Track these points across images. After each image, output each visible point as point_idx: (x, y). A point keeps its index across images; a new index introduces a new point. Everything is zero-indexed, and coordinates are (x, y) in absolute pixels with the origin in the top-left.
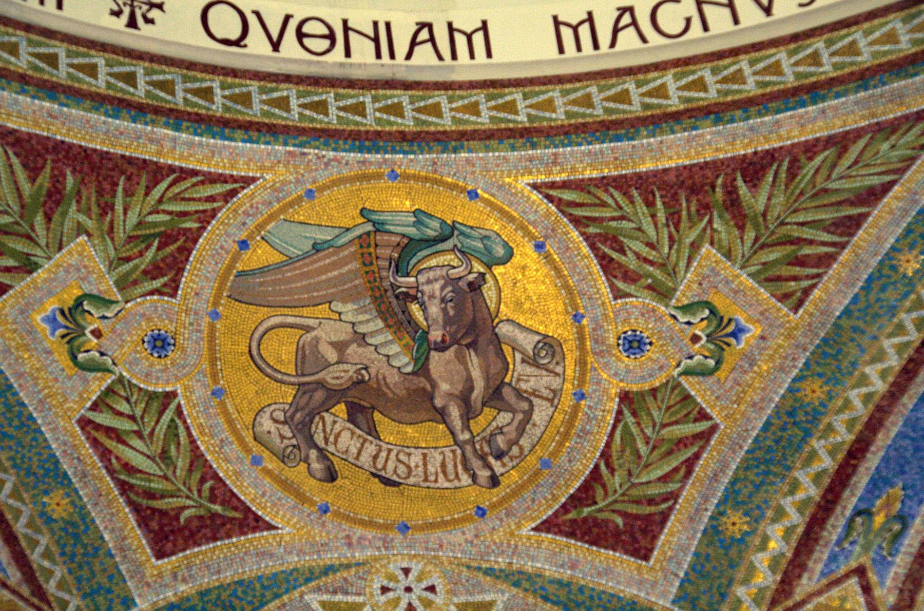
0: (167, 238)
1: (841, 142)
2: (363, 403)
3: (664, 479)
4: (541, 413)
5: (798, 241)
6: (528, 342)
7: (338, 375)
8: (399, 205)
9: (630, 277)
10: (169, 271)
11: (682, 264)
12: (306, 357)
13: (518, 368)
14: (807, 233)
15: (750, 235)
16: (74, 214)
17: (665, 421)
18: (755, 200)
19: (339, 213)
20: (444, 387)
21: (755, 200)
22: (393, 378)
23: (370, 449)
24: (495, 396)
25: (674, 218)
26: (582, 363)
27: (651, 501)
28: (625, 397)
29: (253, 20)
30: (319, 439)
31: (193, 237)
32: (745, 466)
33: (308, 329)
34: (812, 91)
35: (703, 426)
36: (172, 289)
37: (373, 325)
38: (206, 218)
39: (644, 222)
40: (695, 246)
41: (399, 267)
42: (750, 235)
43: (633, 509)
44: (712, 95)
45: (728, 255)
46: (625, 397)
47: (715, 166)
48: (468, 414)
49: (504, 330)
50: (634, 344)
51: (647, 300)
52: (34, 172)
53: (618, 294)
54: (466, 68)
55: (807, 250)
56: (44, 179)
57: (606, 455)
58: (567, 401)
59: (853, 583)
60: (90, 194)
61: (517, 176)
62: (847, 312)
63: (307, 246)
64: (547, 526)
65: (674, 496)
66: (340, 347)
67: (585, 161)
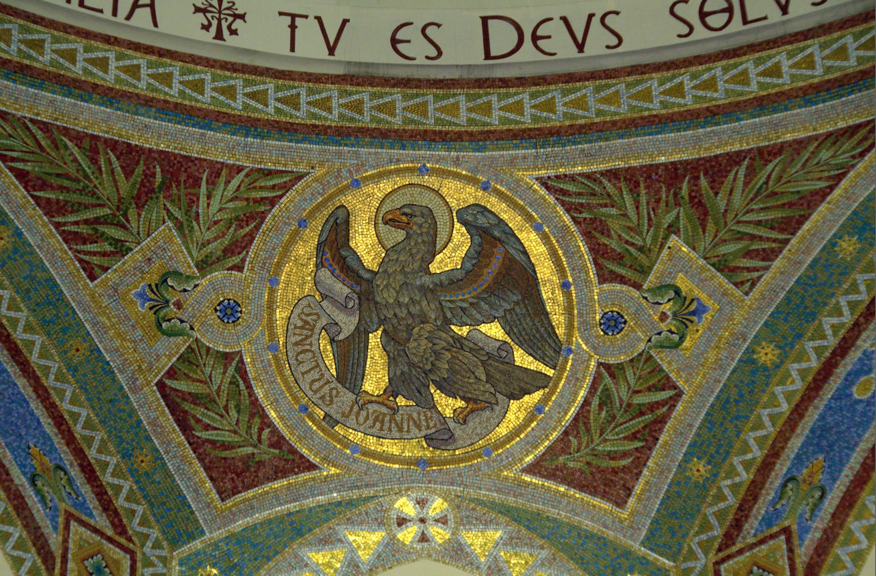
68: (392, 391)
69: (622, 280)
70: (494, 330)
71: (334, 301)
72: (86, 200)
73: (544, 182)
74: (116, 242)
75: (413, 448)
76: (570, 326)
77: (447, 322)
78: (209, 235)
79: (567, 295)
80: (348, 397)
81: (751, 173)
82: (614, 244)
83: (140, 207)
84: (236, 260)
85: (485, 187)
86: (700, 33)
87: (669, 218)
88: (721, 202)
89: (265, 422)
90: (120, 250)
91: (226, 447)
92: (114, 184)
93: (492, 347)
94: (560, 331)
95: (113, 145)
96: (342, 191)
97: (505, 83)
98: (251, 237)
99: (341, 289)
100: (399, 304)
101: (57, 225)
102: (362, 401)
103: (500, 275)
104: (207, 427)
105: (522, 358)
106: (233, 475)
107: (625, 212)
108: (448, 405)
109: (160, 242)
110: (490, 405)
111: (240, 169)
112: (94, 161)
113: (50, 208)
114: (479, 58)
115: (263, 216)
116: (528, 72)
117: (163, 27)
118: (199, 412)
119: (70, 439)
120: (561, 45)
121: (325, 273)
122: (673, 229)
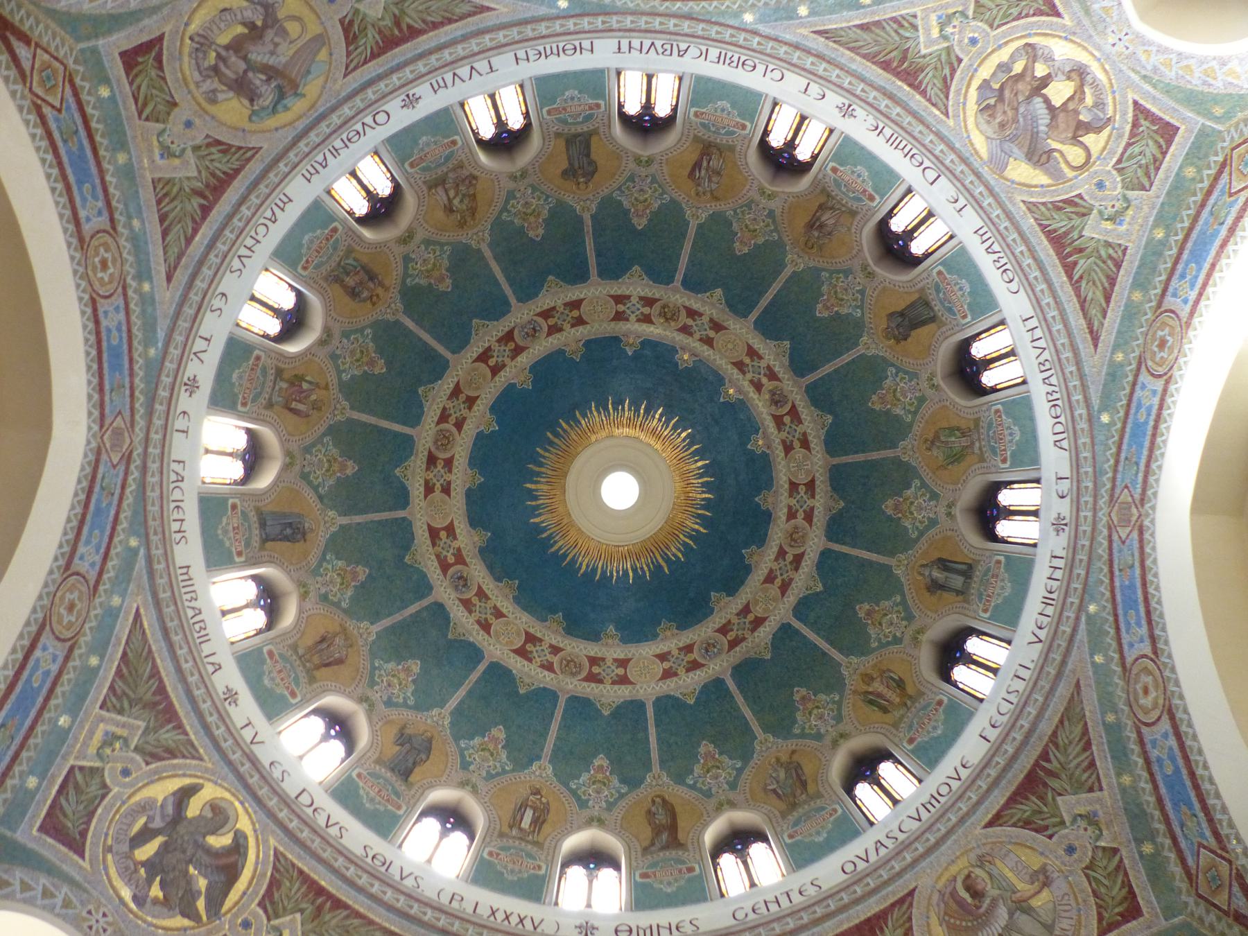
0: (355, 37)
1: (189, 241)
2: (255, 32)
3: (139, 87)
5: (172, 201)
6: (221, 96)
7: (270, 34)
8: (297, 106)
9: (208, 145)
10: (347, 26)
12: (283, 32)
13: (216, 84)
14: (172, 206)
15: (187, 190)
16: (388, 22)
17: (156, 107)
18: (196, 202)
19: (311, 88)
20: (233, 59)
21: (196, 202)
22: (251, 48)
23: (239, 17)
24: (215, 69)
25: (213, 175)
26: (199, 104)
27: (136, 76)
28: (175, 104)
29: (373, 125)
30: (259, 8)
31: (348, 45)
32: (119, 114)
33: (291, 42)
34: (211, 246)
35: (144, 116)
36: (342, 21)
37: (272, 61)
38: (348, 54)
39: (222, 164)
40: (200, 172)
41: (279, 87)
42: (187, 190)
43: (140, 67)
44: (235, 220)
45: (188, 178)
46: (175, 104)
47: (216, 200)
48: (219, 56)
49: (231, 94)
51: (198, 142)
52: (409, 27)
53: (207, 136)
54: (305, 167)
55: (167, 200)
56: (405, 28)
57: (164, 79)
58: (192, 87)
59: (57, 104)
60: (387, 33)
61: (269, 146)
62: (137, 192)
63: (312, 70)
64: (161, 38)
65: (131, 84)
66: (276, 45)
67: (254, 168)
68: (143, 864)
69: (266, 911)
70: (202, 883)
73: (275, 850)
75: (126, 894)
76: (230, 910)
77: (190, 861)
79: (242, 897)
80: (125, 848)
81: (347, 917)
82: (276, 896)
85: (255, 831)
86: (369, 860)
87: (304, 906)
88: (327, 917)
89: (88, 823)
90: (121, 712)
91: (65, 815)
92: (146, 691)
93: (195, 888)
94: (224, 910)
96: (209, 780)
97: (293, 811)
99: (170, 810)
100: (182, 837)
102: (129, 856)
103: (227, 867)
104: (67, 800)
105: (201, 904)
106: (52, 826)
107: (294, 889)
108: (156, 891)
109: (135, 725)
110: (170, 908)
113: (119, 673)
117: (214, 677)
118: (72, 792)
119: (26, 738)
122: (302, 911)
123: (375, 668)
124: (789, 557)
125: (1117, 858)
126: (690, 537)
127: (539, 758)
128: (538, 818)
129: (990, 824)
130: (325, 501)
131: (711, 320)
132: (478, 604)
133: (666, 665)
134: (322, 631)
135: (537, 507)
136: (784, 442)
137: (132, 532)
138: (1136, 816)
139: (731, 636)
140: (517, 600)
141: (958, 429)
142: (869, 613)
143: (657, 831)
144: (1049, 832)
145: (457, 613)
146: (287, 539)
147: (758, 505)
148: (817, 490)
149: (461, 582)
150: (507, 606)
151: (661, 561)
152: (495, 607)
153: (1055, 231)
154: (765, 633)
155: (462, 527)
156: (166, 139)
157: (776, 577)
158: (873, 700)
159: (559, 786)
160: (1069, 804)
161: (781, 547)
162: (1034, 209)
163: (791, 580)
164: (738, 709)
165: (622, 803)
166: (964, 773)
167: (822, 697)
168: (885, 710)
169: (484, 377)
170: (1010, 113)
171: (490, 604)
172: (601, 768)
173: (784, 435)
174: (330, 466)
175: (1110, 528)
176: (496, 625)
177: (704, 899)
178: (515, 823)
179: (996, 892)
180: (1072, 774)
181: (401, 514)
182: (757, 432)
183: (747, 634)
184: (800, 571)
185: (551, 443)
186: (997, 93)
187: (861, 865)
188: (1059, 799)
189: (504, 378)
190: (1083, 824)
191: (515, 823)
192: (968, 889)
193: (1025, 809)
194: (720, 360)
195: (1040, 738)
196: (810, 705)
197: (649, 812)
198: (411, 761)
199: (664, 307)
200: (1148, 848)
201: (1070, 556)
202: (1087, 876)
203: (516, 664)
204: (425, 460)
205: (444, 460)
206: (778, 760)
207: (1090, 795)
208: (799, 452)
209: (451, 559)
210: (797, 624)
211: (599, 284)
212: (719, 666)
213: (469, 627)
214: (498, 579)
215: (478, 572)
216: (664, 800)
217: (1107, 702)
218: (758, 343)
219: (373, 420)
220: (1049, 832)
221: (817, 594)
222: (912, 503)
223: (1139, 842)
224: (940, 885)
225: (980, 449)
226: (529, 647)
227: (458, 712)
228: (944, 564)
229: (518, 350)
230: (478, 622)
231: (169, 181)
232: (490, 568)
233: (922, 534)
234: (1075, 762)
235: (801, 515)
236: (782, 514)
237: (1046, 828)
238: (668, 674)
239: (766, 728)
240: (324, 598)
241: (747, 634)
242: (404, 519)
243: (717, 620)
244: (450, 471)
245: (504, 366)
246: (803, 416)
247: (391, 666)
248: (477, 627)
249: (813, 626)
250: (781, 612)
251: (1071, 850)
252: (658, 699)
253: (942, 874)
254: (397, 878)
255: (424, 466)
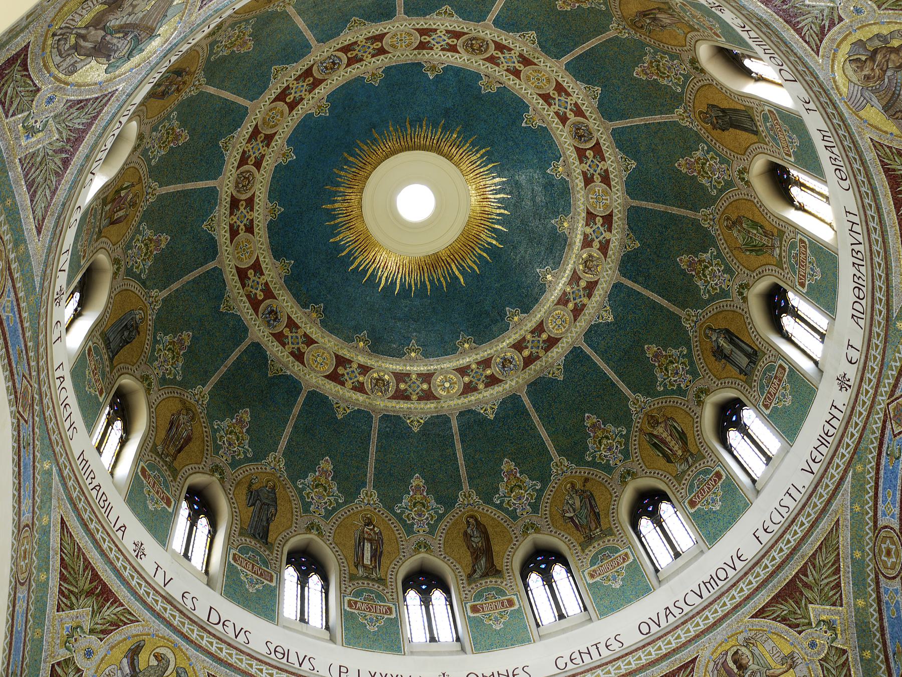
1: (53, 193)
4: (58, 59)
11: (59, 127)
15: (50, 152)
22: (111, 17)
24: (76, 47)
26: (59, 80)
37: (130, 20)
40: (60, 133)
46: (39, 90)
48: (79, 36)
50: (50, 100)
55: (33, 170)
57: (29, 76)
71: (122, 673)
72: (74, 582)
74: (72, 603)
78: (100, 622)
83: (86, 596)
84: (102, 636)
86: (273, 656)
92: (84, 583)
95: (93, 569)
97: (210, 633)
98: (112, 631)
101: (60, 585)
109: (83, 614)
111: (123, 605)
112: (84, 571)
113: (63, 578)
114: (206, 620)
115: (119, 626)
116: (217, 634)
120: (230, 631)
121: (125, 661)
123: (216, 431)
124: (583, 284)
125: (845, 657)
126: (485, 250)
127: (364, 484)
128: (376, 550)
129: (755, 616)
130: (148, 283)
131: (521, 56)
132: (290, 335)
133: (466, 379)
134: (169, 417)
135: (336, 226)
136: (584, 174)
137: (45, 456)
138: (863, 630)
139: (526, 353)
140: (324, 324)
141: (762, 227)
142: (656, 355)
143: (476, 555)
144: (800, 629)
145: (274, 349)
146: (128, 343)
147: (554, 228)
148: (615, 225)
149: (273, 315)
150: (315, 332)
151: (457, 273)
152: (305, 335)
153: (894, 170)
154: (558, 353)
155: (267, 262)
156: (31, 122)
157: (568, 301)
158: (657, 445)
159: (383, 510)
160: (816, 611)
161: (575, 272)
162: (879, 147)
163: (584, 305)
164: (534, 428)
165: (442, 525)
166: (739, 565)
167: (610, 427)
168: (669, 461)
169: (282, 113)
170: (877, 72)
171: (300, 332)
172: (418, 487)
173: (585, 167)
174: (147, 249)
175: (885, 415)
176: (309, 353)
177: (529, 641)
178: (359, 563)
179: (755, 667)
180: (823, 589)
181: (211, 265)
182: (558, 159)
183: (541, 353)
184: (593, 299)
185: (347, 162)
186: (870, 54)
187: (654, 628)
188: (810, 606)
189: (300, 111)
190: (825, 628)
191: (359, 563)
192: (735, 662)
193: (783, 609)
194: (525, 89)
195: (803, 557)
196: (600, 434)
197: (465, 533)
198: (264, 519)
199: (471, 39)
200: (867, 654)
201: (848, 413)
202: (822, 665)
203: (331, 389)
204: (228, 206)
205: (245, 200)
206: (573, 486)
207: (833, 608)
208: (598, 186)
209: (260, 296)
210: (588, 350)
211: (405, 20)
212: (515, 383)
213: (285, 360)
214: (305, 306)
215: (286, 303)
216: (476, 520)
217: (857, 540)
218: (568, 82)
219: (179, 187)
220: (800, 629)
221: (608, 324)
222: (706, 267)
223: (862, 649)
224: (714, 657)
225: (780, 255)
226: (341, 370)
227: (289, 452)
228: (730, 336)
229: (317, 83)
230: (292, 353)
231: (33, 155)
232: (296, 296)
233: (712, 299)
234: (826, 581)
235: (596, 244)
236: (578, 239)
237: (798, 626)
238: (469, 389)
239: (561, 452)
240: (163, 381)
241: (541, 353)
242: (215, 269)
243: (513, 337)
244: (252, 210)
245: (302, 99)
246: (606, 155)
247: (227, 422)
248: (291, 358)
249: (603, 355)
250: (572, 335)
251: (813, 645)
252: (461, 414)
253: (717, 648)
254: (297, 665)
255: (228, 213)
